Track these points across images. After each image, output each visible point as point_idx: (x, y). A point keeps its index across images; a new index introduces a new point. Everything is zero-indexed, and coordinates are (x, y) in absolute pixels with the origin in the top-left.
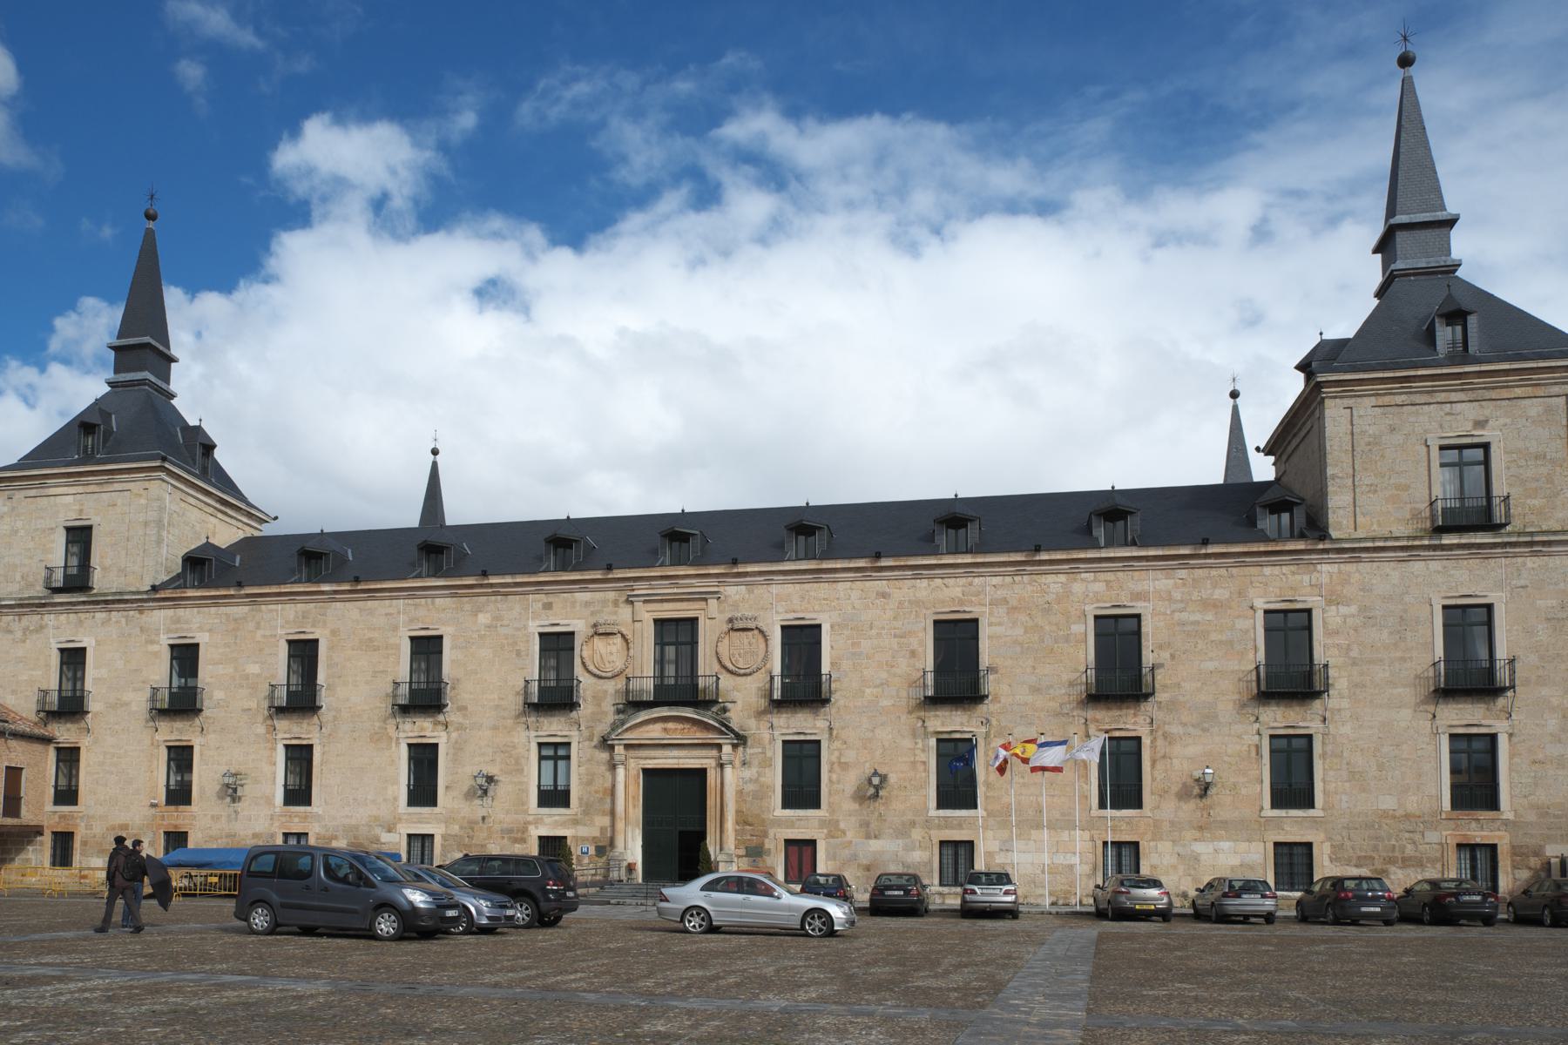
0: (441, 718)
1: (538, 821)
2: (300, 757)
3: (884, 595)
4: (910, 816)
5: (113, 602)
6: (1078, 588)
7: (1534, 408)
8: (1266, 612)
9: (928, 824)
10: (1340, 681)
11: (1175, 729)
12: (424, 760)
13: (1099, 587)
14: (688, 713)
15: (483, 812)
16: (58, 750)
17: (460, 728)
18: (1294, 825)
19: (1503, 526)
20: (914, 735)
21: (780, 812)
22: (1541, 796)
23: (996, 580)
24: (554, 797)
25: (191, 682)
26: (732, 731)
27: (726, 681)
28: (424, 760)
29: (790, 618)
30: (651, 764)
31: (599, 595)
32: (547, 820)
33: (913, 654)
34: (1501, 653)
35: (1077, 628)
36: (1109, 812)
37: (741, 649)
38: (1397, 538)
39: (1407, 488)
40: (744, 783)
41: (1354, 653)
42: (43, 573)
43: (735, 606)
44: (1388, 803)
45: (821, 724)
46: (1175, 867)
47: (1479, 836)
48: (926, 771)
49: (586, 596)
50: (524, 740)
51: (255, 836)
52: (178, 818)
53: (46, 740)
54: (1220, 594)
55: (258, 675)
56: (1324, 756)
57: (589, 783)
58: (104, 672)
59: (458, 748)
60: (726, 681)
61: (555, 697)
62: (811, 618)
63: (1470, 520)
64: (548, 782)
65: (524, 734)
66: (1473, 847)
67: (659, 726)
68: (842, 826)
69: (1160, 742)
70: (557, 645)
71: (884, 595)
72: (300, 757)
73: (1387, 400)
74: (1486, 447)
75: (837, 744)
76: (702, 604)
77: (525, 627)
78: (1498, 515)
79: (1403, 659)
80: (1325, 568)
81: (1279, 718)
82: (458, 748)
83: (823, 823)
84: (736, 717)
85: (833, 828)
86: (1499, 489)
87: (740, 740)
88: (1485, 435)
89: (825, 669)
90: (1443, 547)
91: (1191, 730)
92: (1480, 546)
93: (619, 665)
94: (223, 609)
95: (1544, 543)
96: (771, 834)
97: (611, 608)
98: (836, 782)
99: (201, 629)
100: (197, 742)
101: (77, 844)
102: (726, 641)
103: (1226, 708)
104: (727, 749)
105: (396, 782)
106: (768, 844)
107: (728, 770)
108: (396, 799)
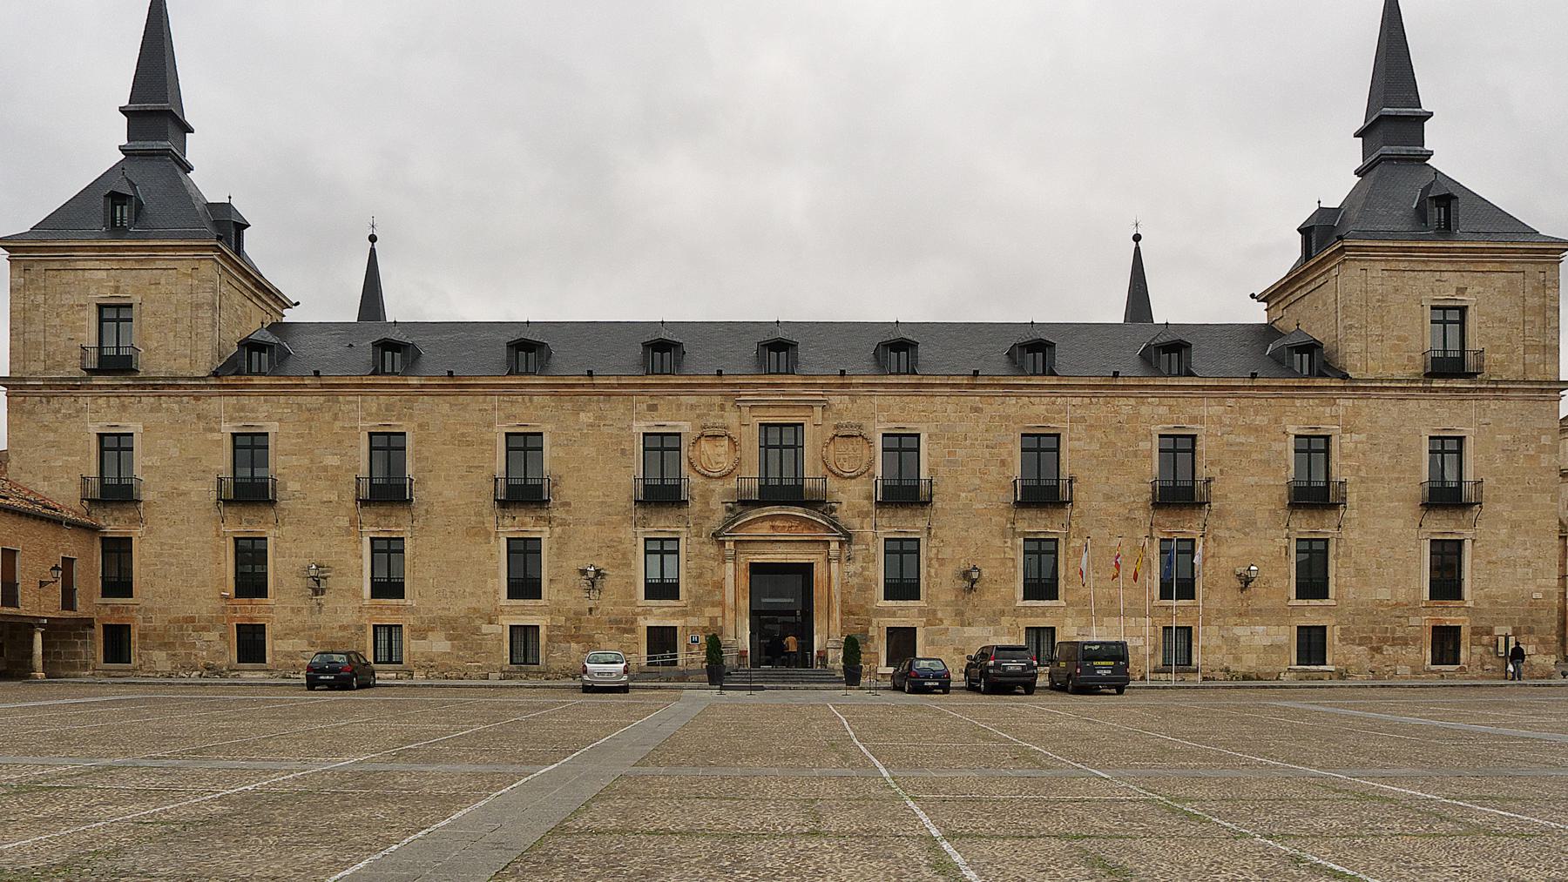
0: (544, 514)
1: (647, 613)
2: (387, 550)
3: (977, 410)
4: (1000, 606)
5: (163, 386)
6: (1144, 410)
7: (1499, 280)
8: (1297, 436)
9: (1016, 612)
10: (1352, 499)
11: (1222, 533)
12: (524, 553)
13: (1163, 410)
14: (798, 512)
15: (591, 604)
16: (104, 540)
17: (564, 523)
18: (1312, 613)
19: (1475, 374)
20: (1004, 534)
21: (882, 603)
22: (1493, 589)
23: (1076, 401)
24: (662, 590)
26: (841, 529)
27: (833, 484)
28: (524, 553)
29: (891, 427)
31: (704, 399)
32: (656, 611)
33: (1003, 463)
34: (1469, 476)
36: (1174, 603)
37: (847, 456)
38: (1399, 381)
39: (1405, 339)
40: (848, 581)
41: (1362, 474)
42: (77, 353)
43: (839, 414)
44: (1384, 594)
45: (921, 523)
46: (1219, 647)
47: (1449, 620)
48: (1015, 567)
49: (693, 400)
50: (631, 535)
51: (343, 628)
52: (252, 610)
54: (1261, 420)
55: (338, 467)
56: (1337, 556)
57: (700, 576)
58: (155, 460)
59: (561, 544)
60: (833, 484)
61: (661, 495)
62: (911, 428)
64: (655, 575)
65: (631, 530)
67: (767, 524)
68: (940, 615)
69: (1211, 543)
70: (661, 445)
72: (387, 550)
73: (1393, 265)
75: (934, 542)
76: (807, 412)
77: (630, 428)
78: (1471, 363)
79: (1398, 479)
80: (1341, 402)
81: (1304, 525)
82: (561, 544)
83: (921, 612)
84: (844, 515)
85: (931, 618)
86: (1473, 343)
87: (847, 538)
89: (924, 475)
90: (1431, 390)
91: (1235, 533)
92: (1458, 390)
93: (727, 465)
94: (300, 399)
95: (1503, 390)
96: (875, 621)
97: (716, 411)
98: (938, 578)
99: (269, 418)
100: (271, 534)
101: (135, 637)
102: (831, 447)
103: (1262, 517)
104: (834, 546)
105: (496, 575)
106: (873, 632)
107: (834, 565)
108: (496, 592)
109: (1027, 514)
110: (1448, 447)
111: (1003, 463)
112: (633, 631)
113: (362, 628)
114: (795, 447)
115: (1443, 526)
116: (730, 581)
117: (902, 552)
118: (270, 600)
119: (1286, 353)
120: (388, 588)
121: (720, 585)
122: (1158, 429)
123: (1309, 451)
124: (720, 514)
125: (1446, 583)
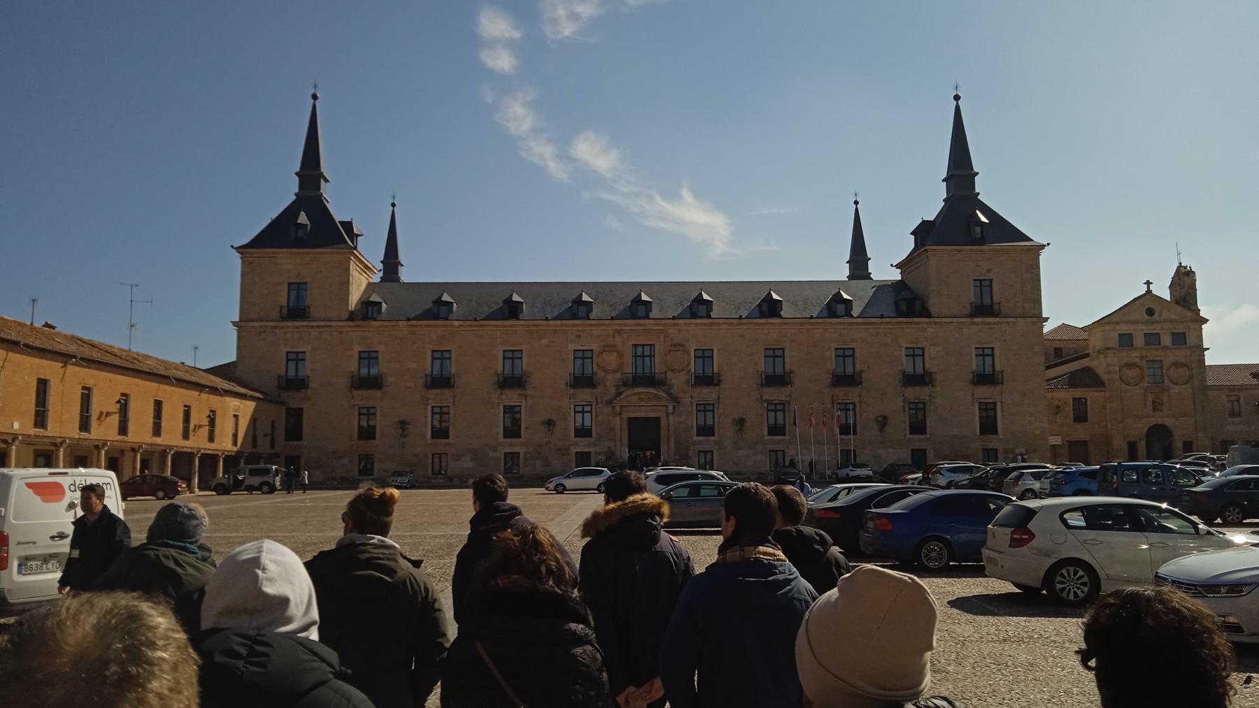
1: (575, 445)
2: (441, 412)
14: (652, 390)
16: (288, 409)
18: (919, 441)
21: (696, 438)
24: (582, 432)
25: (373, 371)
30: (633, 415)
33: (756, 364)
35: (828, 354)
51: (416, 455)
53: (283, 403)
60: (670, 375)
61: (583, 381)
63: (984, 310)
66: (988, 450)
67: (636, 398)
71: (743, 336)
72: (441, 412)
74: (991, 281)
83: (716, 443)
84: (675, 390)
88: (990, 276)
106: (691, 453)
107: (671, 418)
109: (767, 390)
110: (985, 353)
111: (756, 364)
112: (568, 454)
113: (426, 456)
114: (650, 356)
115: (984, 392)
116: (618, 427)
117: (705, 408)
118: (377, 441)
119: (905, 299)
120: (440, 433)
121: (613, 429)
122: (834, 346)
123: (914, 356)
124: (613, 391)
125: (989, 426)
